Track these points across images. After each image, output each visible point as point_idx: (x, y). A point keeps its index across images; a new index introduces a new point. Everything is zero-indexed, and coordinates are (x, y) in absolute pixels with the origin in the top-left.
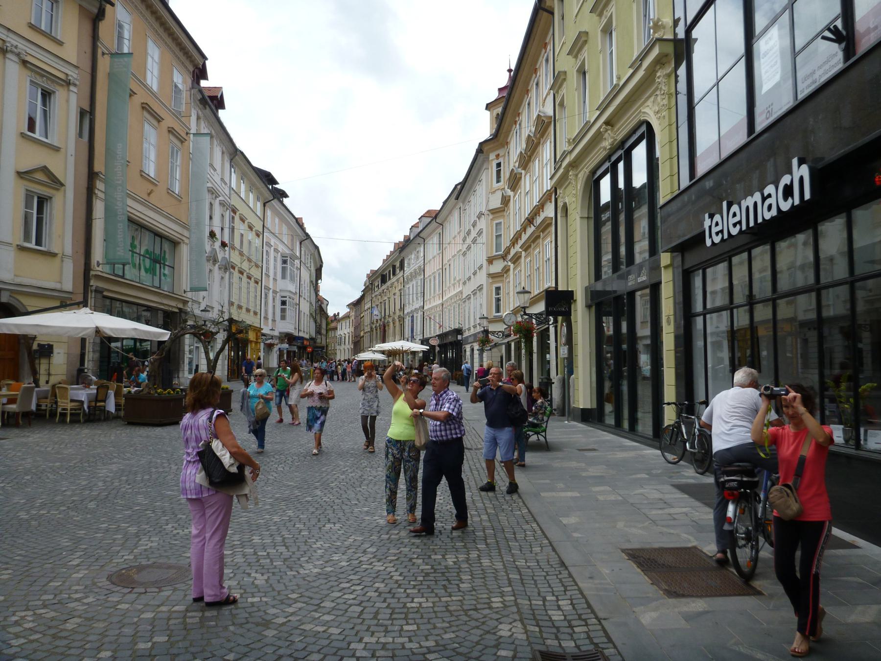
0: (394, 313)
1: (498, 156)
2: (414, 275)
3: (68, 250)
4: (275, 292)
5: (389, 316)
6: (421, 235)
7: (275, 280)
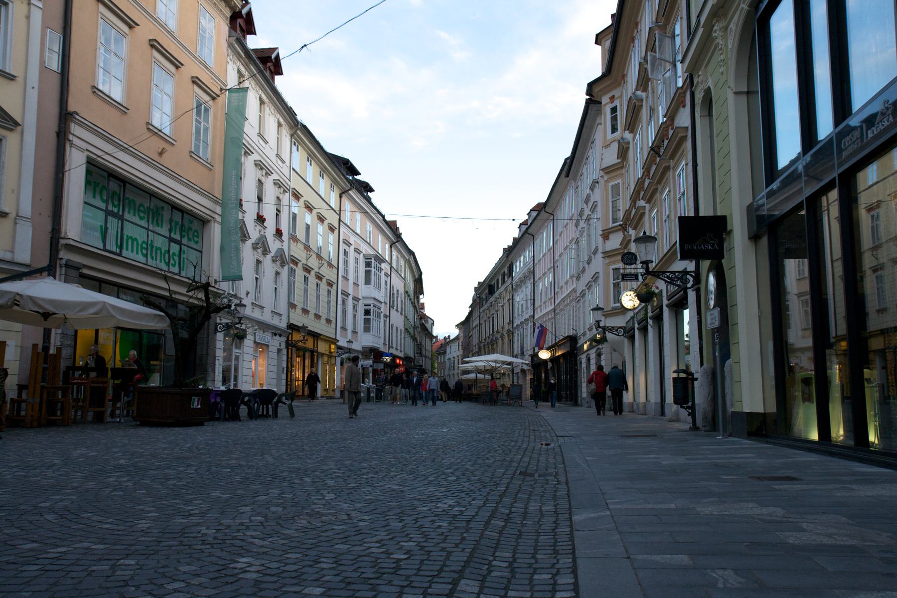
0: (503, 328)
1: (612, 99)
2: (523, 281)
3: (26, 209)
4: (356, 299)
5: (498, 332)
6: (530, 231)
7: (356, 284)
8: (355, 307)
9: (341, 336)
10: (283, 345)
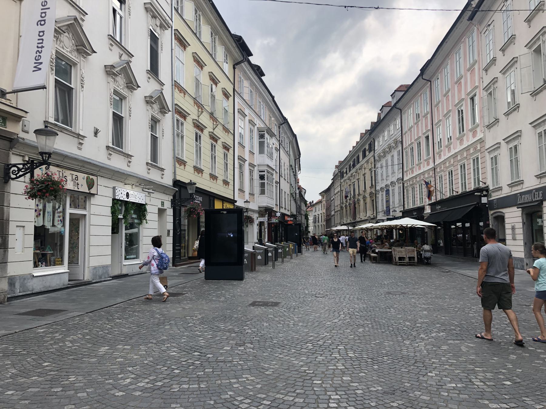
0: (365, 191)
4: (251, 165)
5: (359, 195)
6: (398, 106)
8: (251, 172)
9: (239, 197)
10: (168, 205)
